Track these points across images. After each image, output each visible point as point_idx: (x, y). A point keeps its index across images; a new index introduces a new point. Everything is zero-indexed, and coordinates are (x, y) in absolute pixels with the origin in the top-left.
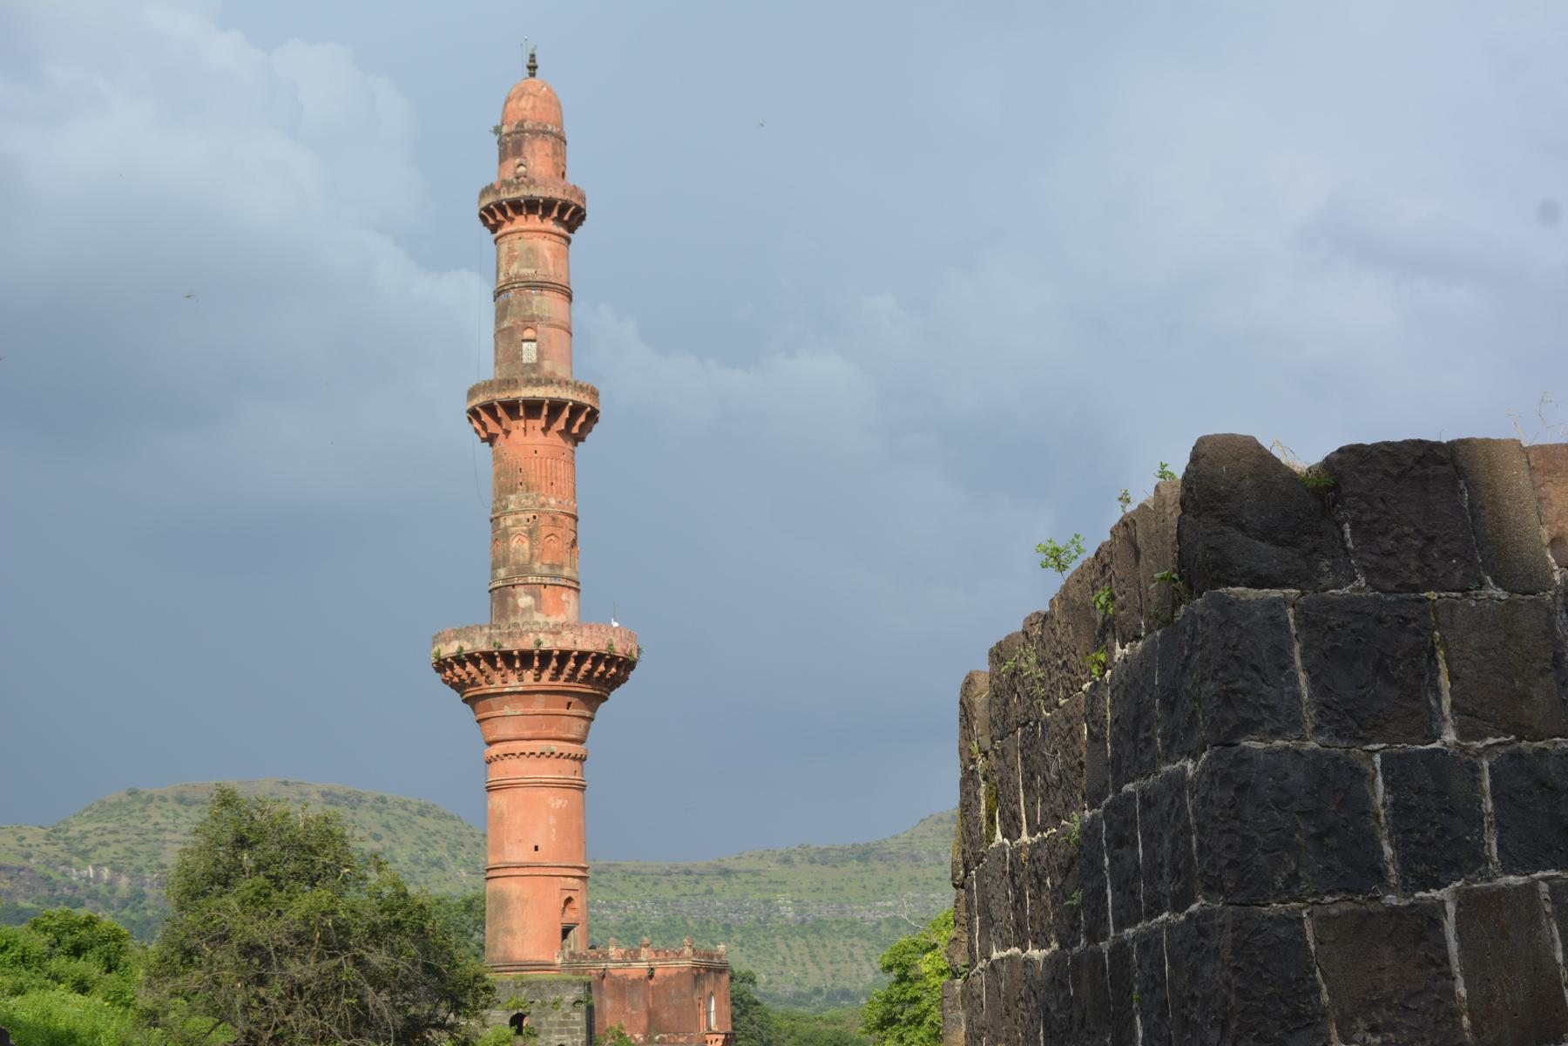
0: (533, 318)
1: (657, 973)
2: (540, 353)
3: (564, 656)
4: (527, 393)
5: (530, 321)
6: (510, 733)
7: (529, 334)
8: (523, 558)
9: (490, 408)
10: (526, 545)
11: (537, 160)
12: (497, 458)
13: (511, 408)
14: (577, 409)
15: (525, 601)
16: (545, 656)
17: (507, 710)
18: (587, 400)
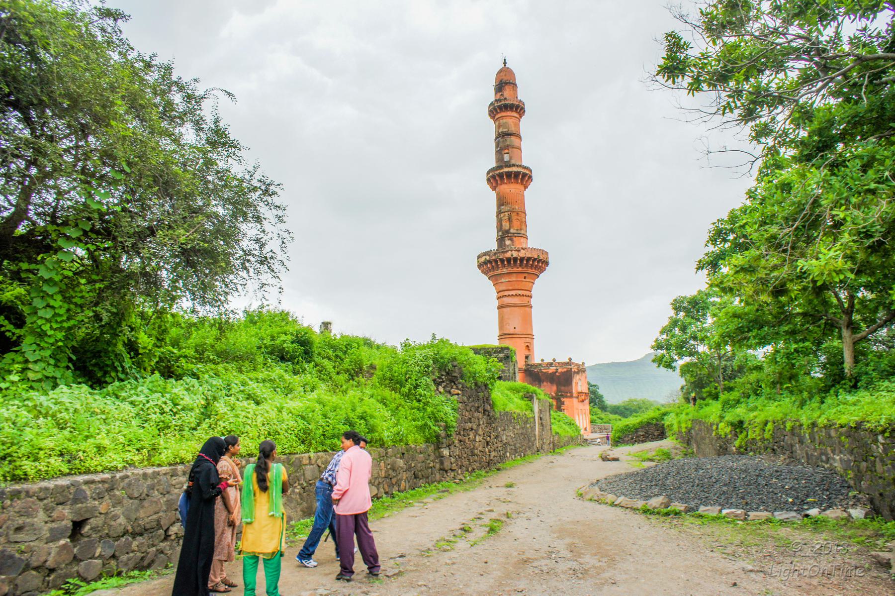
0: (508, 146)
1: (559, 371)
2: (511, 158)
3: (522, 259)
4: (506, 170)
5: (507, 147)
6: (504, 288)
7: (506, 151)
8: (507, 228)
9: (493, 177)
10: (508, 224)
11: (507, 93)
12: (498, 195)
13: (501, 176)
14: (524, 175)
15: (508, 242)
16: (515, 259)
17: (503, 280)
18: (528, 172)
